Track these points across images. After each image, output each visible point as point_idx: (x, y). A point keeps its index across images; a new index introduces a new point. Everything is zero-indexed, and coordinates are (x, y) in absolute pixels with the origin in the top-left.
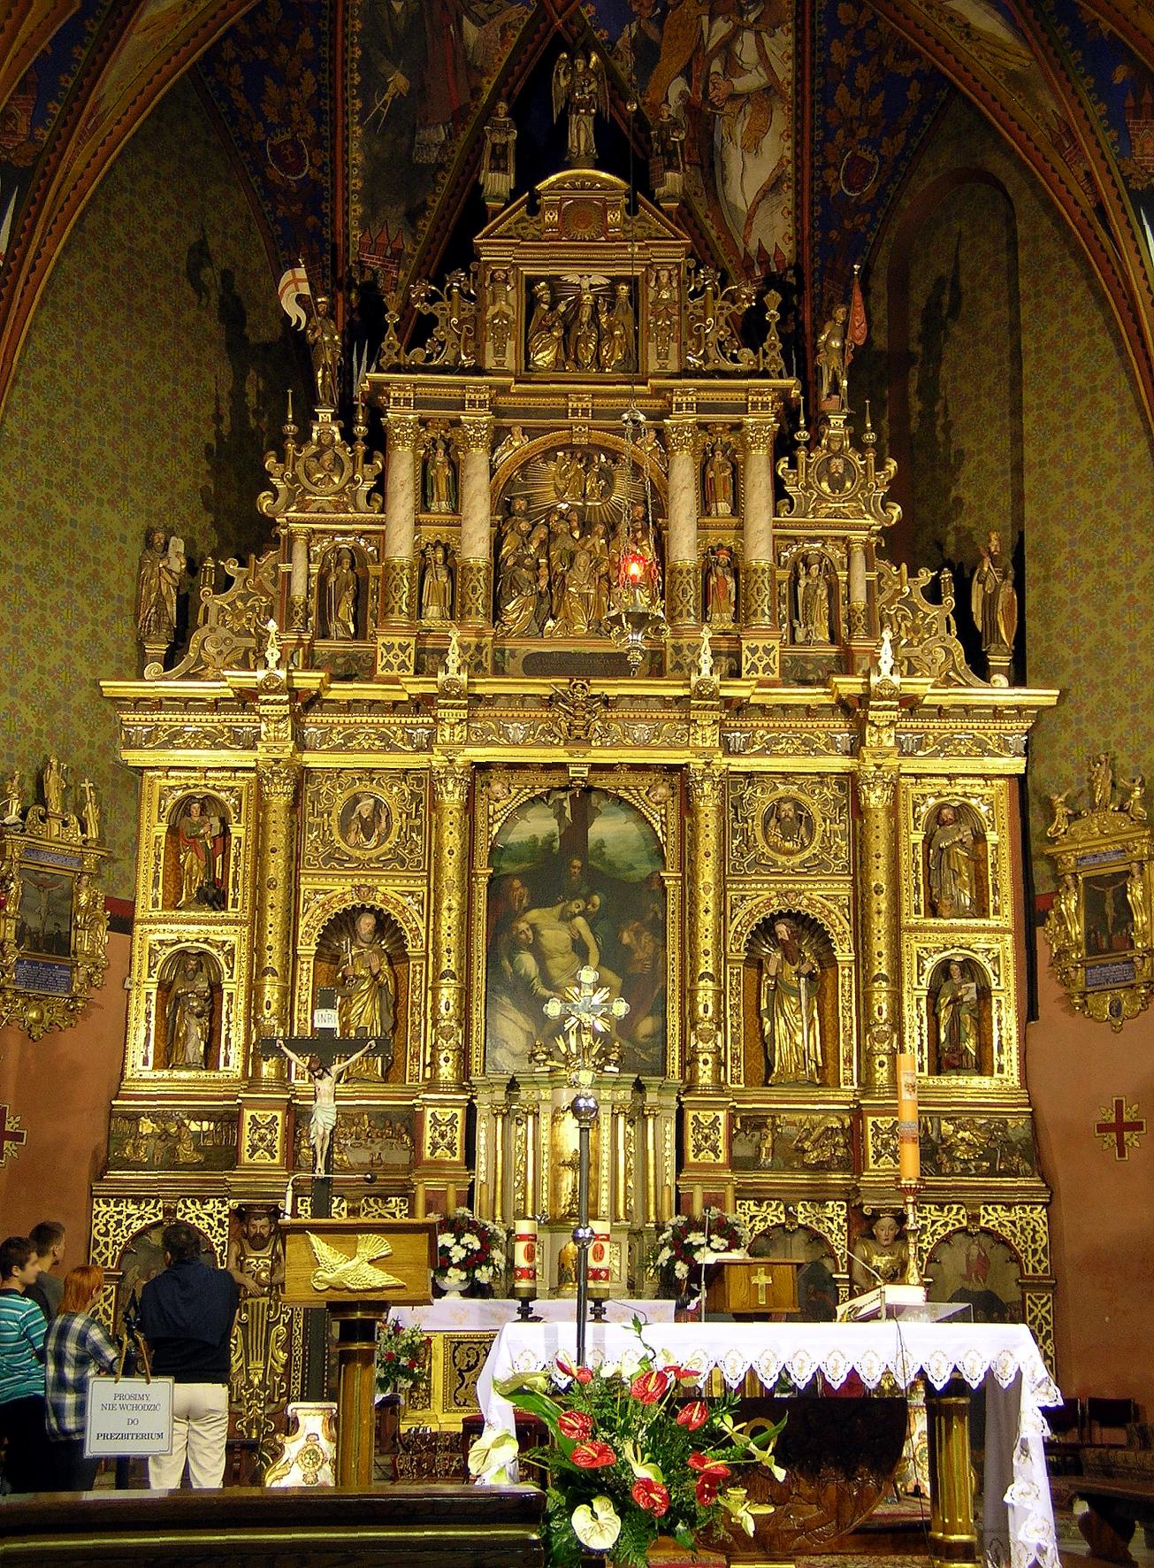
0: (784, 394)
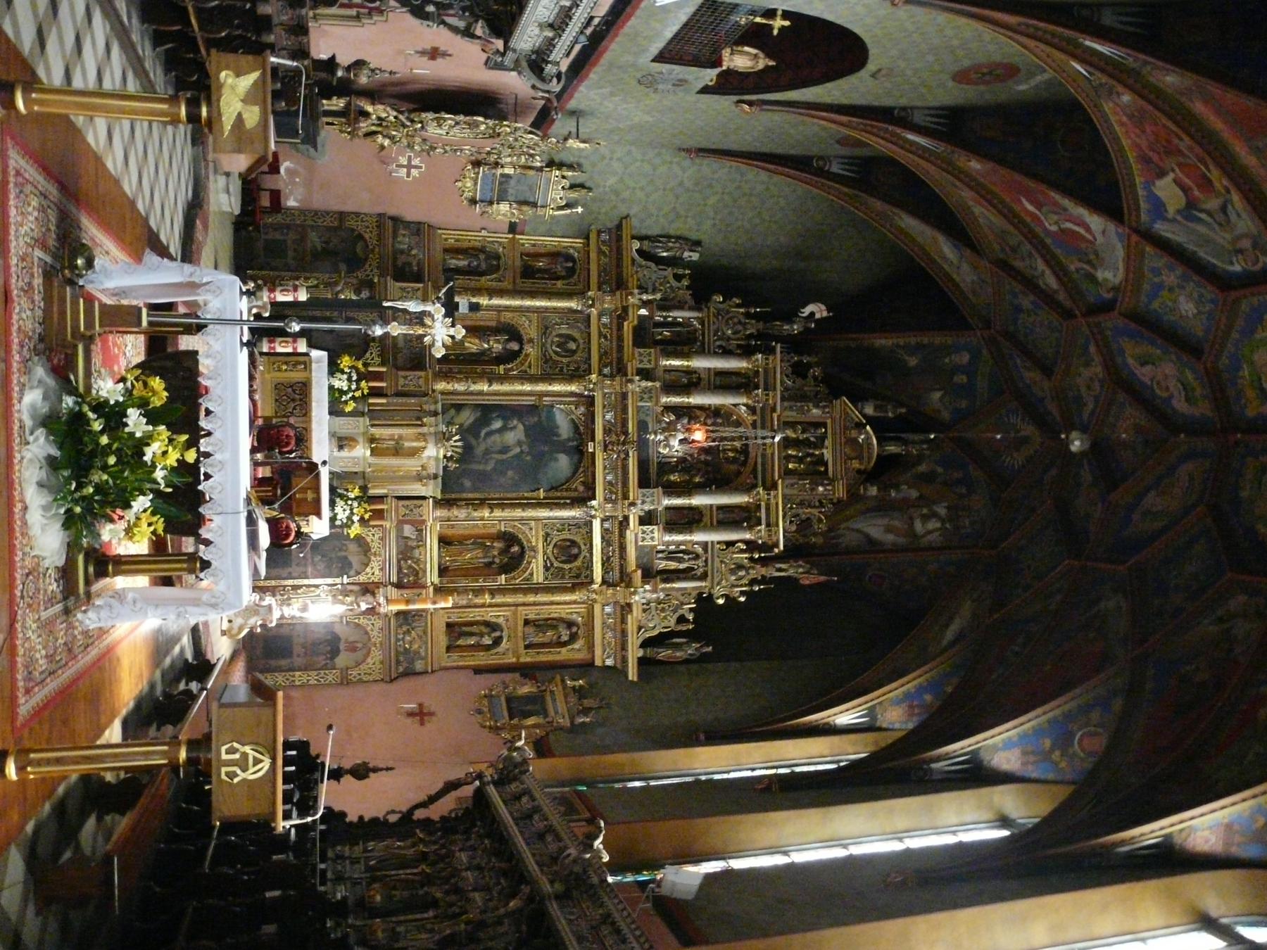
0: (776, 545)
